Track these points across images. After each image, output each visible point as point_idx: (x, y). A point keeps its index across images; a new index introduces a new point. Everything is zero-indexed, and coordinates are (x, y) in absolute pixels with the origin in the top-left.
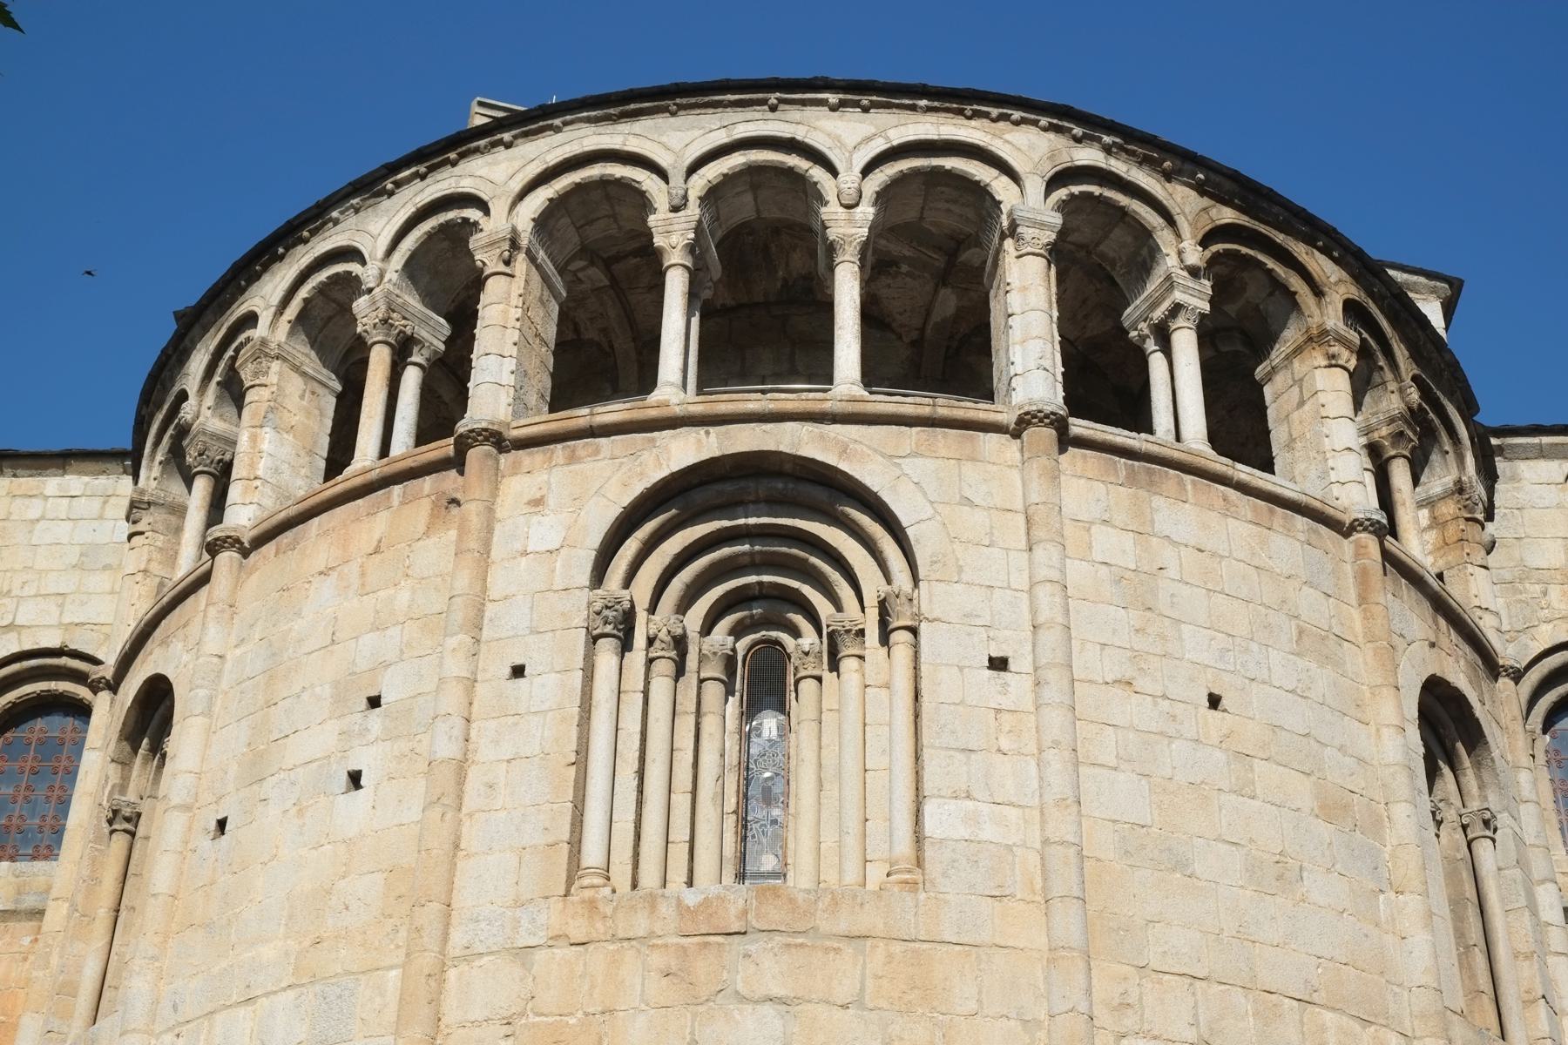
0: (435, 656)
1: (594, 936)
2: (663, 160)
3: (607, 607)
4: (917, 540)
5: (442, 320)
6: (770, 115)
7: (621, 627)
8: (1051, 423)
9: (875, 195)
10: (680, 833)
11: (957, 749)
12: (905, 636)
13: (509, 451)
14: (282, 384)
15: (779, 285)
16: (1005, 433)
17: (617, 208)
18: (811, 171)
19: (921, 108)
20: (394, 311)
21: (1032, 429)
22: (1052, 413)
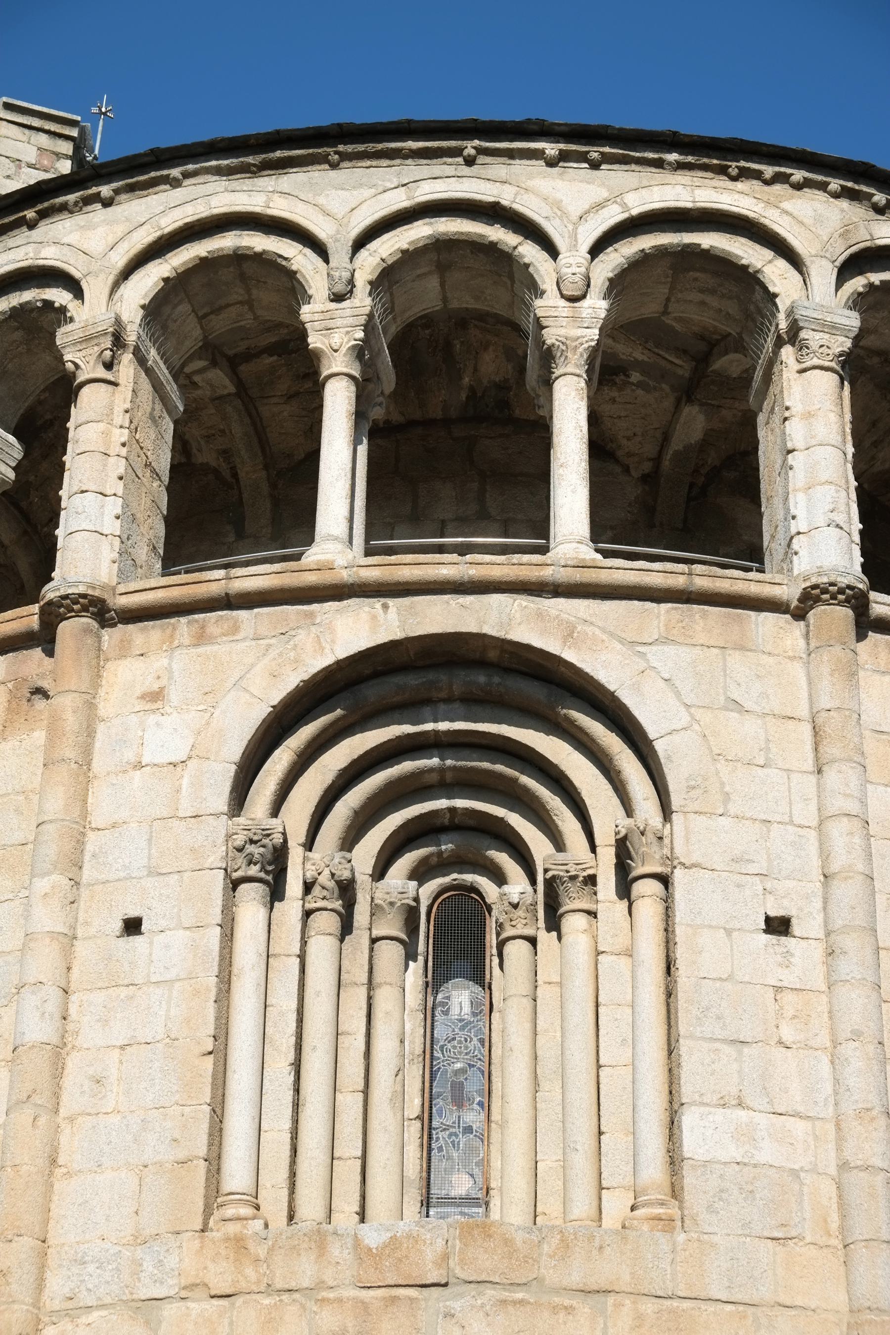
0: (17, 902)
1: (243, 1285)
2: (321, 229)
3: (252, 842)
4: (669, 758)
5: (11, 438)
6: (466, 170)
7: (270, 868)
8: (847, 600)
9: (607, 283)
10: (349, 1147)
11: (724, 1041)
12: (654, 887)
13: (114, 625)
15: (463, 396)
16: (785, 612)
17: (254, 292)
18: (520, 249)
19: (670, 164)
21: (821, 609)
22: (849, 587)
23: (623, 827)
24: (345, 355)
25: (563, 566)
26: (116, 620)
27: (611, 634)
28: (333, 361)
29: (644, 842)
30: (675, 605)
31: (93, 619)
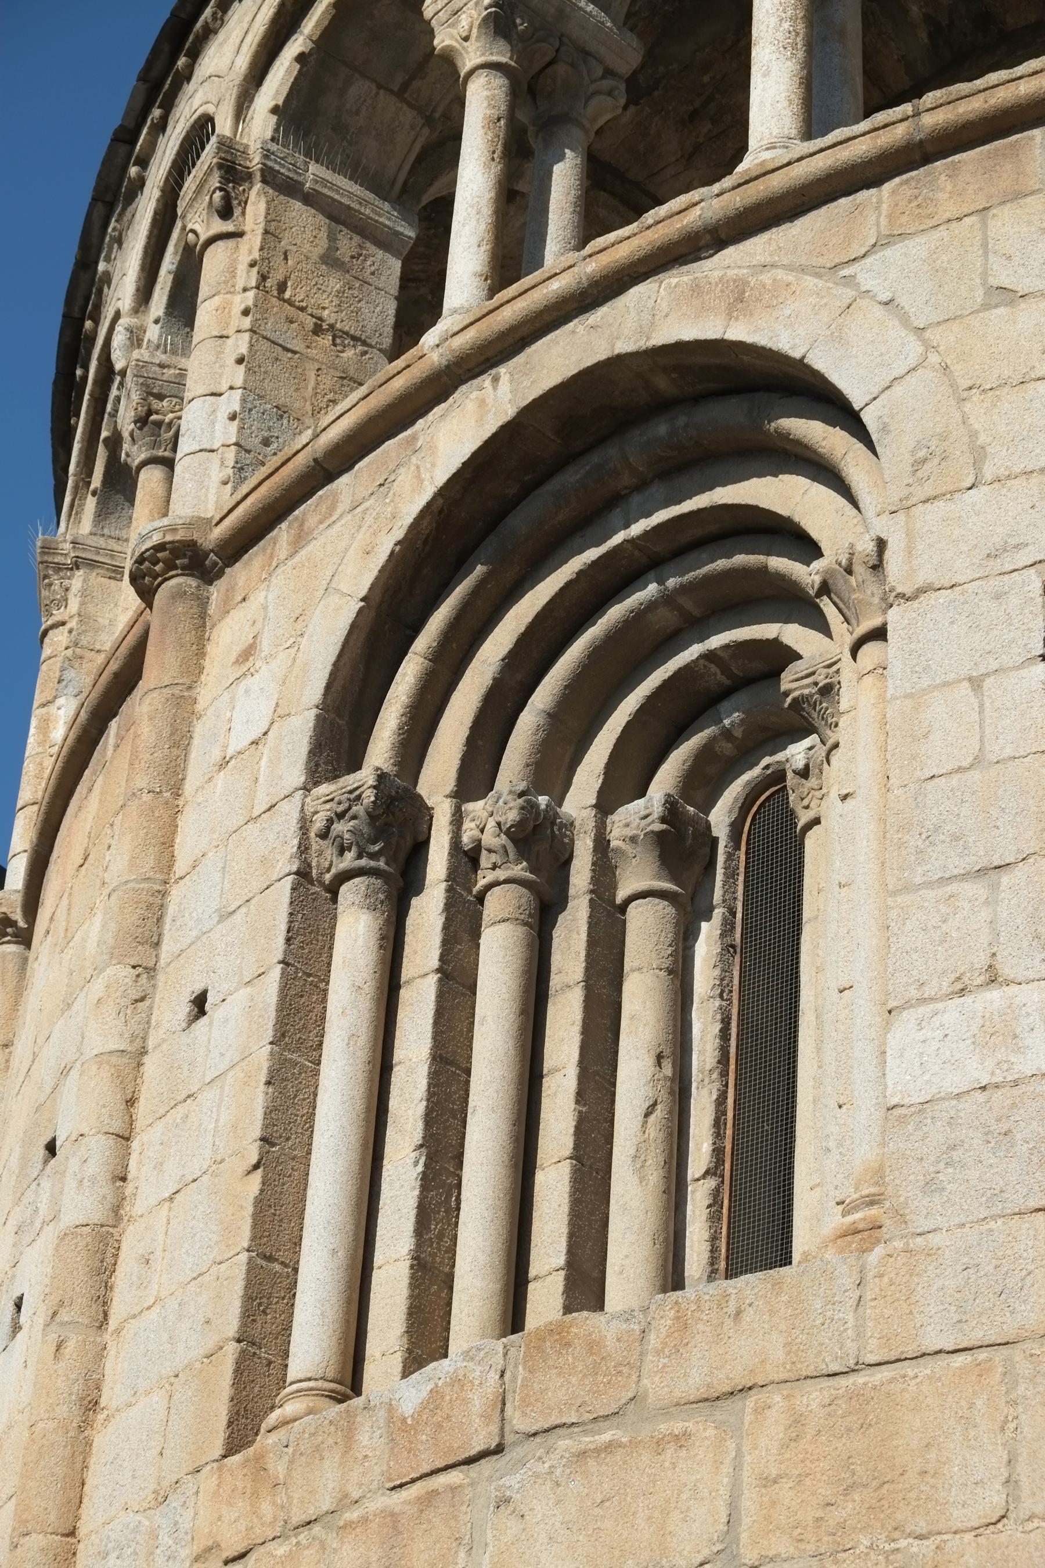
3: (340, 816)
4: (885, 429)
11: (964, 877)
13: (220, 574)
14: (91, 608)
15: (923, 36)
20: (160, 397)
23: (817, 573)
24: (478, 39)
25: (718, 195)
26: (221, 564)
27: (803, 270)
28: (465, 55)
29: (854, 584)
30: (905, 177)
31: (187, 575)
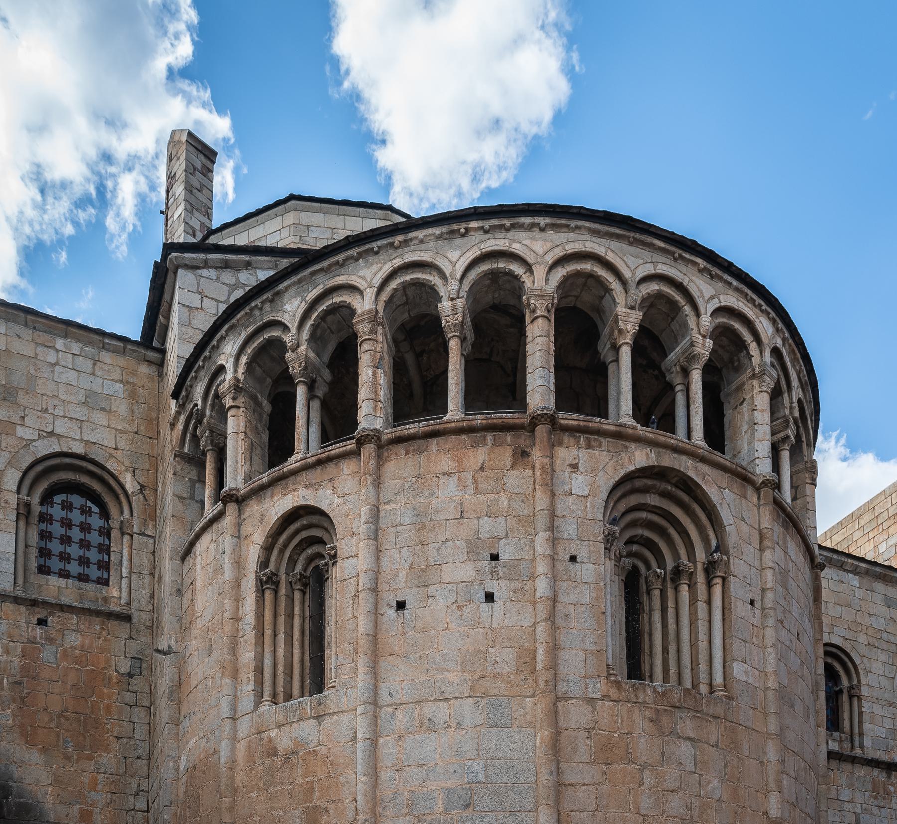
0: (528, 540)
